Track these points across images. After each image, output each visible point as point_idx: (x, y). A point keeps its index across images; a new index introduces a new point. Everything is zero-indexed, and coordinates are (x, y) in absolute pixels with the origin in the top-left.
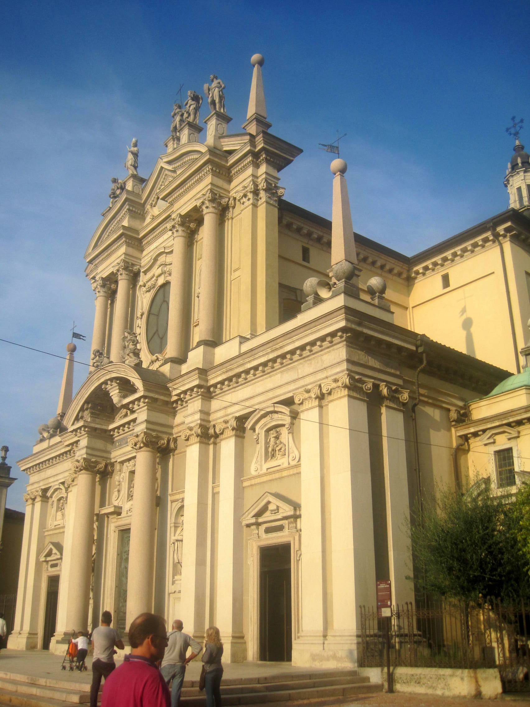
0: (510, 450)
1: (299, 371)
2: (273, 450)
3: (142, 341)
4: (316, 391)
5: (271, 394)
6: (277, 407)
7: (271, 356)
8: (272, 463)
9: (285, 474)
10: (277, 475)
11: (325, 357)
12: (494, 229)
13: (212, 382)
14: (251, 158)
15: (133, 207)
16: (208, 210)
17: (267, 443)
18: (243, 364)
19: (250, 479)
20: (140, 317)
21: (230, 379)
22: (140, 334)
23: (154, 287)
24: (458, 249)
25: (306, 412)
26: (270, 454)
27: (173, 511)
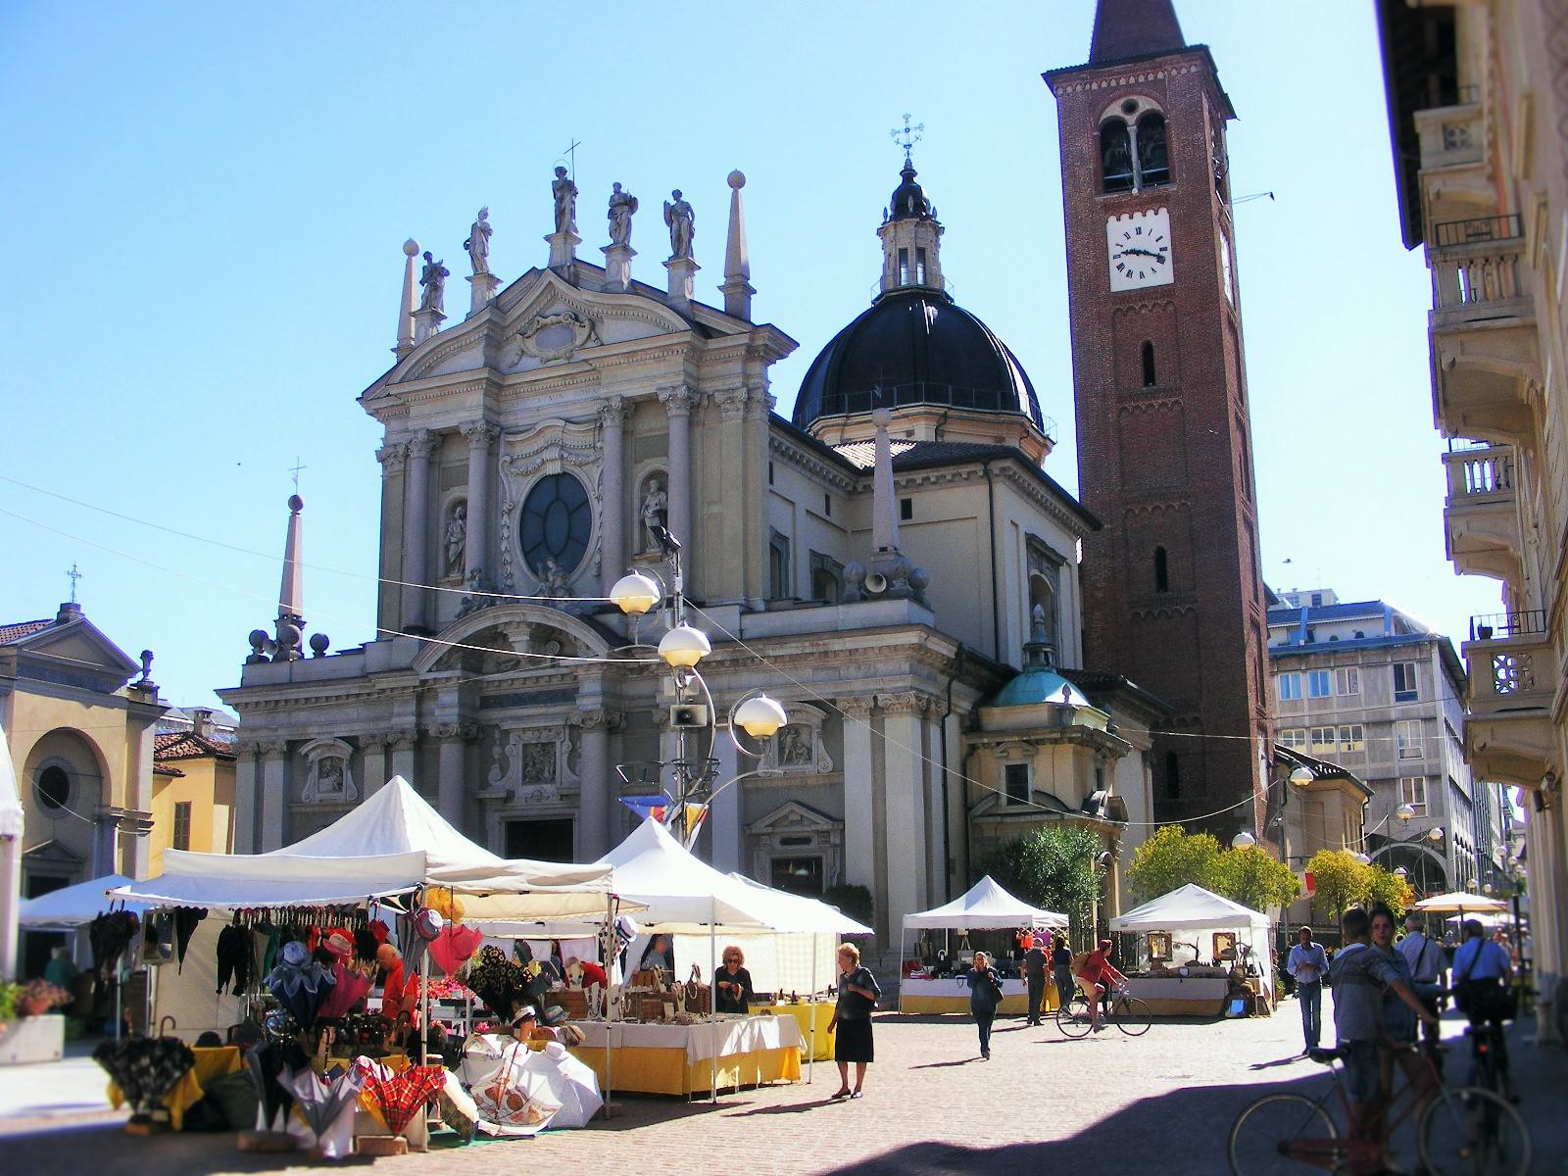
0: (1024, 767)
6: (805, 707)
12: (986, 464)
15: (493, 330)
16: (679, 412)
24: (933, 474)
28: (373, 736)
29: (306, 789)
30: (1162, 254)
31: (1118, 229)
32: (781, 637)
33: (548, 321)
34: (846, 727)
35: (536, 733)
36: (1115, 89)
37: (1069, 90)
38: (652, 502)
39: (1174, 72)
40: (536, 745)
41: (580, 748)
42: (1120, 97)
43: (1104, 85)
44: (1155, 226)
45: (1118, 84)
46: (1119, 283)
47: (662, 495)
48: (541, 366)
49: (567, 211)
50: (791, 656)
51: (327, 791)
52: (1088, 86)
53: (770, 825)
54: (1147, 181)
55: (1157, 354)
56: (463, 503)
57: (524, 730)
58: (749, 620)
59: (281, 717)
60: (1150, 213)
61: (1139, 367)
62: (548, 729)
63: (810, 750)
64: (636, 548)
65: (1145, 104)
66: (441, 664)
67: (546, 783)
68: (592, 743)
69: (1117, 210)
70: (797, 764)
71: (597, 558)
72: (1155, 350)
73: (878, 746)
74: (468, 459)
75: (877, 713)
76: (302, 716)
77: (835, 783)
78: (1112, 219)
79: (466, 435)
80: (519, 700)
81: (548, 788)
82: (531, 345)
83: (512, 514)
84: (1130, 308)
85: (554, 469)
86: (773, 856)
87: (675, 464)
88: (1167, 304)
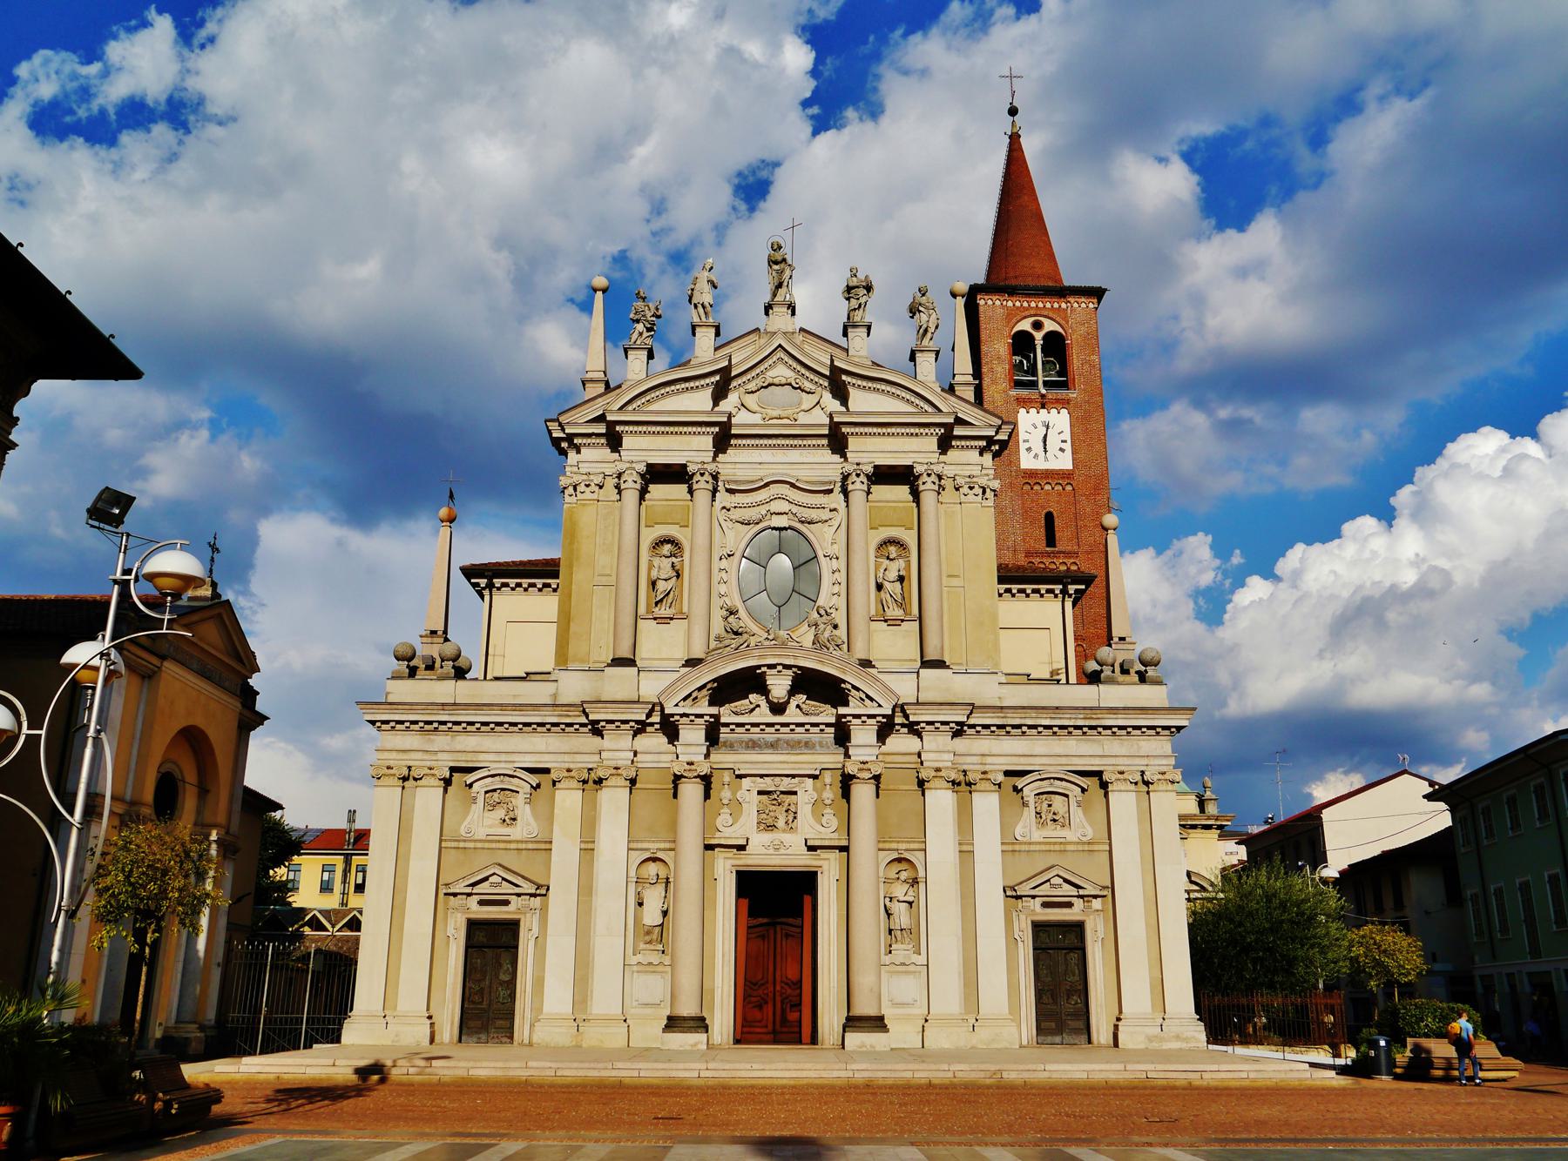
1: (1105, 747)
5: (1063, 761)
9: (1070, 847)
10: (1057, 847)
11: (1142, 743)
13: (972, 721)
14: (985, 444)
19: (1013, 843)
21: (1000, 727)
23: (757, 523)
28: (569, 770)
29: (465, 823)
30: (1064, 446)
31: (1029, 422)
32: (1057, 708)
33: (776, 381)
35: (778, 779)
36: (1026, 309)
37: (990, 302)
39: (1076, 305)
40: (768, 793)
42: (1031, 316)
43: (1018, 304)
44: (1060, 420)
45: (1029, 306)
46: (1027, 462)
47: (901, 563)
48: (762, 422)
49: (785, 284)
51: (491, 826)
52: (1005, 303)
53: (1034, 888)
54: (1046, 384)
55: (1057, 522)
57: (762, 776)
59: (441, 741)
60: (1054, 411)
61: (1043, 531)
62: (793, 776)
64: (873, 612)
65: (1049, 326)
67: (784, 831)
69: (1024, 403)
72: (1056, 520)
73: (1147, 817)
76: (469, 742)
78: (1022, 411)
79: (694, 474)
80: (753, 745)
81: (787, 838)
82: (751, 401)
84: (1038, 483)
88: (1067, 484)
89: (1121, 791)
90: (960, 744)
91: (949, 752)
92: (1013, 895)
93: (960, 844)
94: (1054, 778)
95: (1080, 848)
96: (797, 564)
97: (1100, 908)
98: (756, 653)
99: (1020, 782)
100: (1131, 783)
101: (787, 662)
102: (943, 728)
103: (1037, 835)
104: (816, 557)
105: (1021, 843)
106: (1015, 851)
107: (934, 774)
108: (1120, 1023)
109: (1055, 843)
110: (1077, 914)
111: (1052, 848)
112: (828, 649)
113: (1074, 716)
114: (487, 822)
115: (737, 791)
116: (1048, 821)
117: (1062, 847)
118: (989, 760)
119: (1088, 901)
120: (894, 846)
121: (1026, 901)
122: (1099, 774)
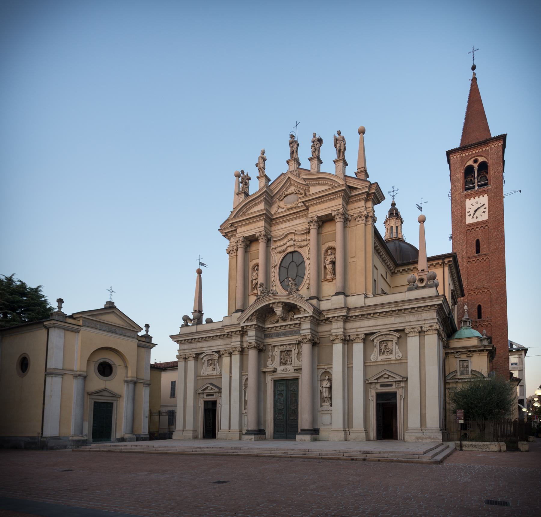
2: (384, 351)
3: (276, 281)
4: (419, 329)
5: (389, 326)
7: (394, 309)
8: (385, 357)
9: (392, 362)
10: (387, 363)
13: (351, 315)
17: (380, 347)
18: (375, 310)
19: (370, 362)
20: (274, 267)
21: (362, 315)
22: (274, 277)
23: (284, 252)
25: (411, 337)
26: (381, 352)
27: (319, 373)
32: (383, 304)
34: (409, 340)
38: (329, 258)
41: (302, 351)
50: (387, 312)
56: (257, 265)
58: (367, 300)
63: (392, 350)
64: (323, 277)
66: (247, 319)
68: (306, 348)
70: (387, 355)
71: (308, 282)
74: (259, 249)
75: (422, 332)
77: (403, 361)
83: (276, 267)
85: (291, 249)
86: (377, 391)
87: (338, 245)
89: (412, 336)
90: (349, 325)
91: (341, 328)
92: (367, 384)
93: (348, 364)
94: (386, 334)
95: (397, 362)
96: (297, 265)
97: (404, 385)
98: (267, 299)
99: (372, 338)
100: (417, 332)
101: (277, 301)
102: (339, 319)
103: (380, 358)
104: (304, 261)
105: (373, 362)
106: (371, 365)
107: (335, 337)
108: (406, 432)
109: (386, 361)
110: (394, 389)
111: (385, 363)
112: (292, 293)
113: (390, 306)
114: (209, 370)
115: (273, 352)
116: (385, 352)
117: (389, 362)
118: (359, 330)
119: (398, 383)
120: (323, 367)
121: (374, 385)
122: (403, 330)
